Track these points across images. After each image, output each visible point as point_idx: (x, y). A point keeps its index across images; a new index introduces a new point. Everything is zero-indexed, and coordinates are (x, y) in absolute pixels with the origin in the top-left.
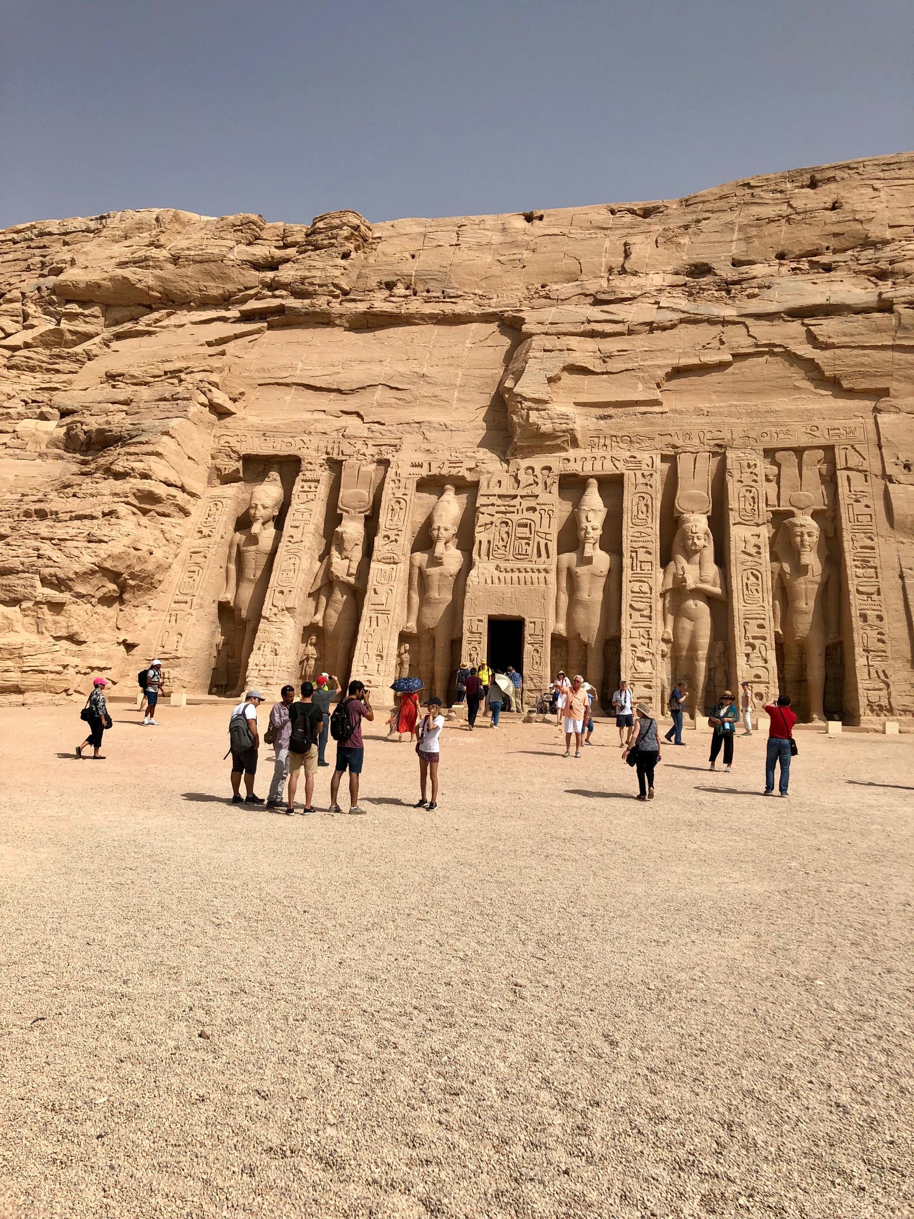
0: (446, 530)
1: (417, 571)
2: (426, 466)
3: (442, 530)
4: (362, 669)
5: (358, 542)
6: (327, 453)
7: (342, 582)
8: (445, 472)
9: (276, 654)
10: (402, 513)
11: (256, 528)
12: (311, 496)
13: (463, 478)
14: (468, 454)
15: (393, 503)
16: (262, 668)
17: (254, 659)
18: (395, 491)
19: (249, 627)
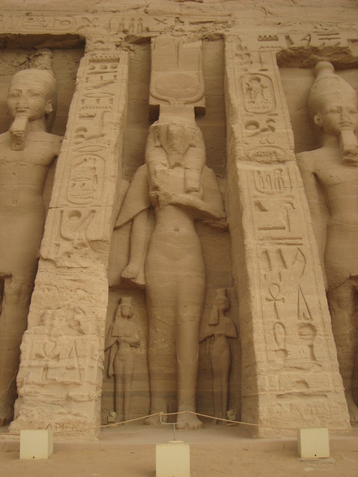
0: (351, 112)
1: (311, 180)
2: (282, 39)
3: (345, 112)
4: (279, 360)
5: (193, 142)
6: (125, 32)
7: (178, 206)
8: (316, 42)
9: (82, 332)
10: (267, 93)
11: (19, 124)
12: (108, 77)
13: (345, 51)
14: (340, 26)
15: (246, 79)
16: (52, 363)
17: (29, 345)
18: (247, 66)
19: (10, 288)
